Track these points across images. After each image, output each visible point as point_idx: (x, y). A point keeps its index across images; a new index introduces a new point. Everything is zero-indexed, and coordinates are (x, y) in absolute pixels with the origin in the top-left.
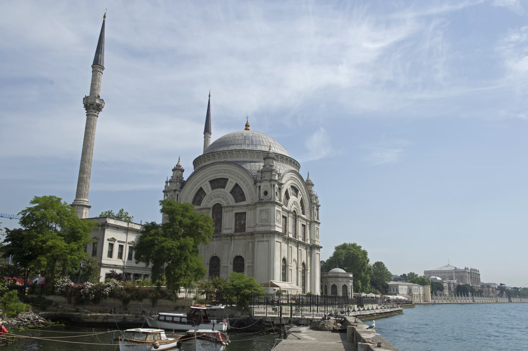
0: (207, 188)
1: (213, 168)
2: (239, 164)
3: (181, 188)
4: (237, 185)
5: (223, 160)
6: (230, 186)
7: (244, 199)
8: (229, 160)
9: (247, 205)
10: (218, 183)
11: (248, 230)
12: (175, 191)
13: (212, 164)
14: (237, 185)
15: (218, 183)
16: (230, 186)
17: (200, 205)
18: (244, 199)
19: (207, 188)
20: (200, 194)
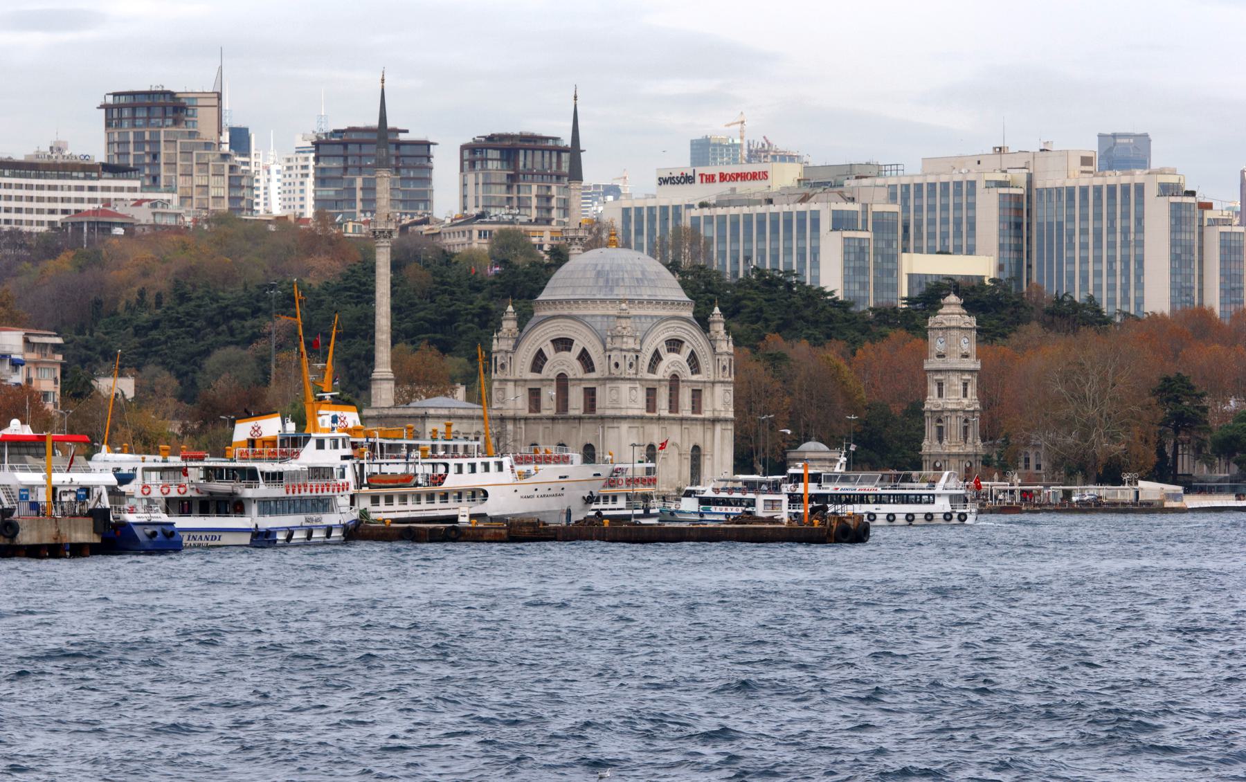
0: (549, 351)
1: (554, 323)
2: (587, 319)
3: (515, 347)
4: (584, 350)
5: (566, 312)
6: (576, 350)
7: (593, 370)
8: (575, 312)
9: (597, 380)
10: (563, 344)
11: (599, 412)
12: (507, 352)
13: (554, 317)
14: (584, 350)
15: (563, 344)
16: (576, 350)
17: (540, 372)
18: (593, 370)
19: (549, 351)
20: (539, 360)
